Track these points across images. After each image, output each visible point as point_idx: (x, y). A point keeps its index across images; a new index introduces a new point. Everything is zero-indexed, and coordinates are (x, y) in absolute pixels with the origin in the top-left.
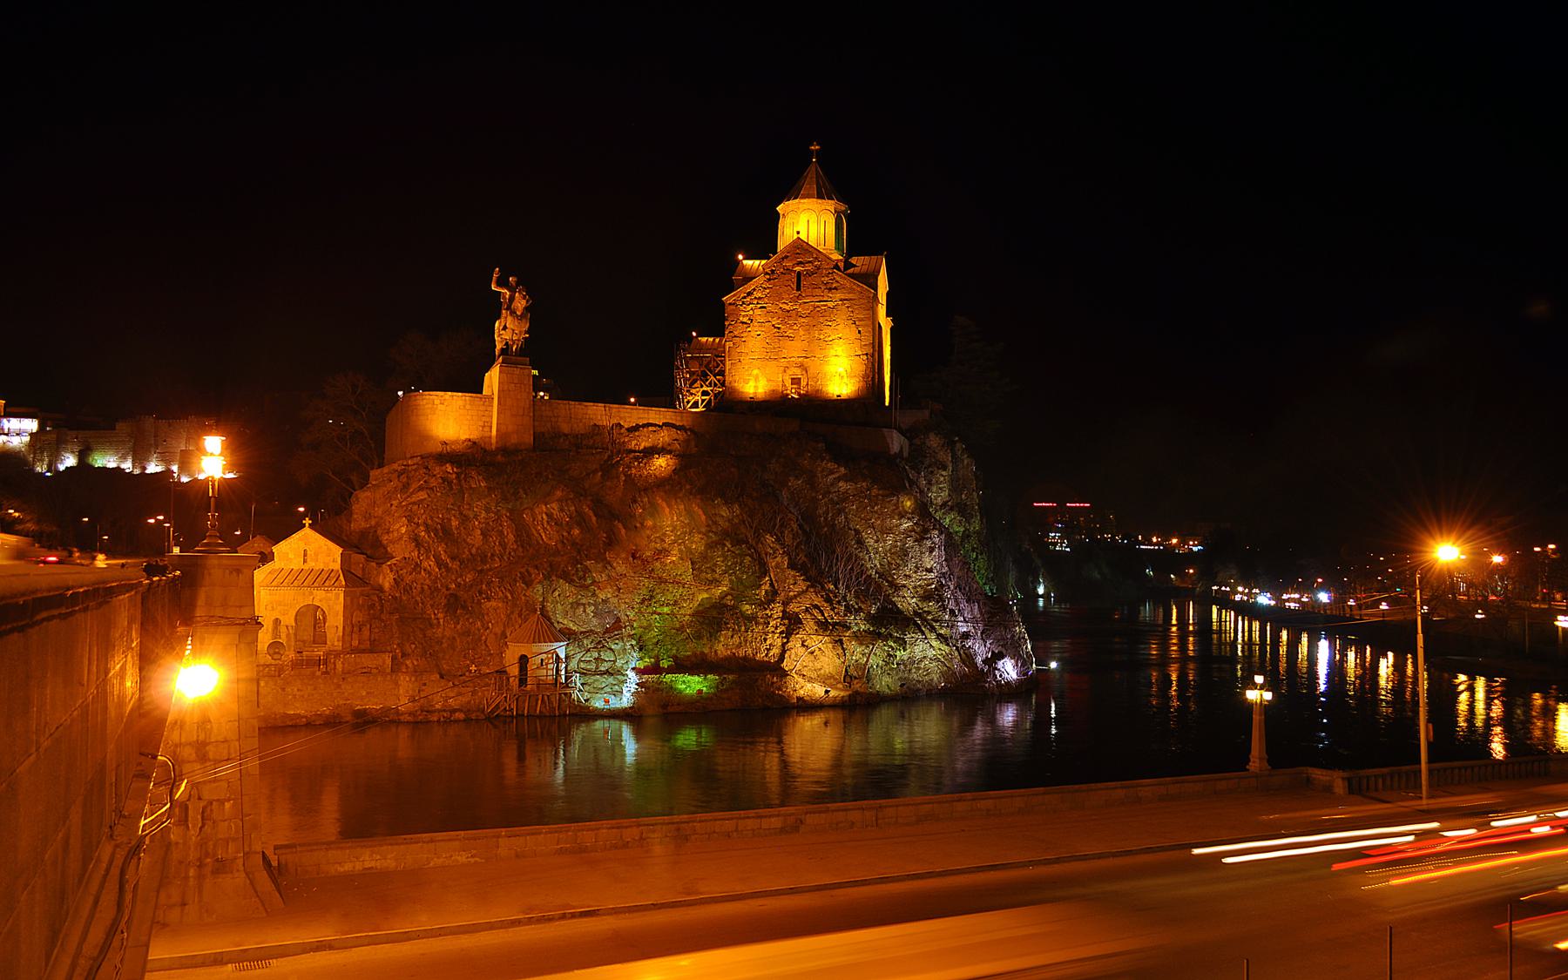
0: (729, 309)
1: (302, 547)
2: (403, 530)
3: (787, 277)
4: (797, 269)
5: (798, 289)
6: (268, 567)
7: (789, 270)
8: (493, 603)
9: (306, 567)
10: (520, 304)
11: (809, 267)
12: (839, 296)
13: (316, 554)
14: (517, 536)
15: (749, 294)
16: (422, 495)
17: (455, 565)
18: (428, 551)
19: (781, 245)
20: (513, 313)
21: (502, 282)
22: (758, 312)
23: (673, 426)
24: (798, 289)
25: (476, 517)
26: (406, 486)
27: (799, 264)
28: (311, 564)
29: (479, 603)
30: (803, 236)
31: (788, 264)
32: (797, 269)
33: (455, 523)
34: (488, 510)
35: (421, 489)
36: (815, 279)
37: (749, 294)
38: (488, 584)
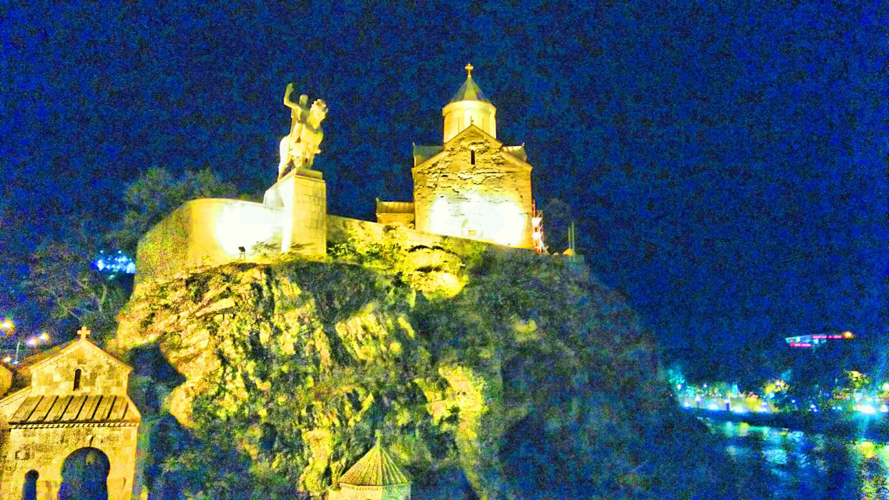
0: (416, 177)
1: (75, 365)
2: (203, 345)
3: (464, 153)
4: (473, 148)
5: (473, 162)
6: (19, 396)
7: (465, 149)
8: (316, 432)
9: (78, 393)
10: (318, 112)
11: (481, 147)
12: (503, 169)
13: (94, 376)
14: (334, 354)
15: (434, 165)
16: (228, 303)
17: (265, 386)
18: (235, 370)
19: (449, 135)
20: (309, 126)
21: (294, 99)
22: (442, 179)
23: (442, 249)
24: (473, 162)
25: (288, 328)
26: (198, 297)
27: (474, 143)
28: (85, 389)
29: (299, 433)
30: (478, 123)
31: (464, 144)
32: (473, 148)
33: (264, 338)
34: (301, 320)
35: (223, 296)
36: (487, 156)
37: (434, 165)
38: (309, 409)
